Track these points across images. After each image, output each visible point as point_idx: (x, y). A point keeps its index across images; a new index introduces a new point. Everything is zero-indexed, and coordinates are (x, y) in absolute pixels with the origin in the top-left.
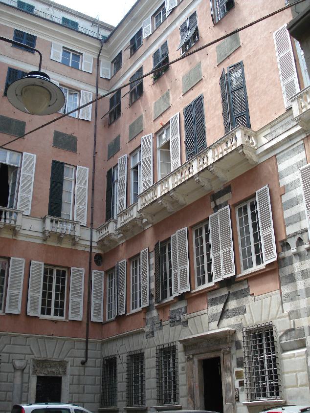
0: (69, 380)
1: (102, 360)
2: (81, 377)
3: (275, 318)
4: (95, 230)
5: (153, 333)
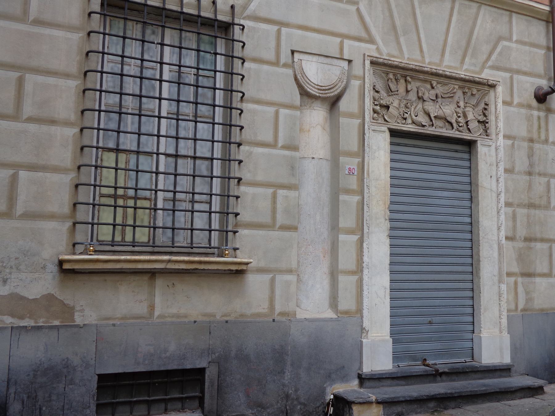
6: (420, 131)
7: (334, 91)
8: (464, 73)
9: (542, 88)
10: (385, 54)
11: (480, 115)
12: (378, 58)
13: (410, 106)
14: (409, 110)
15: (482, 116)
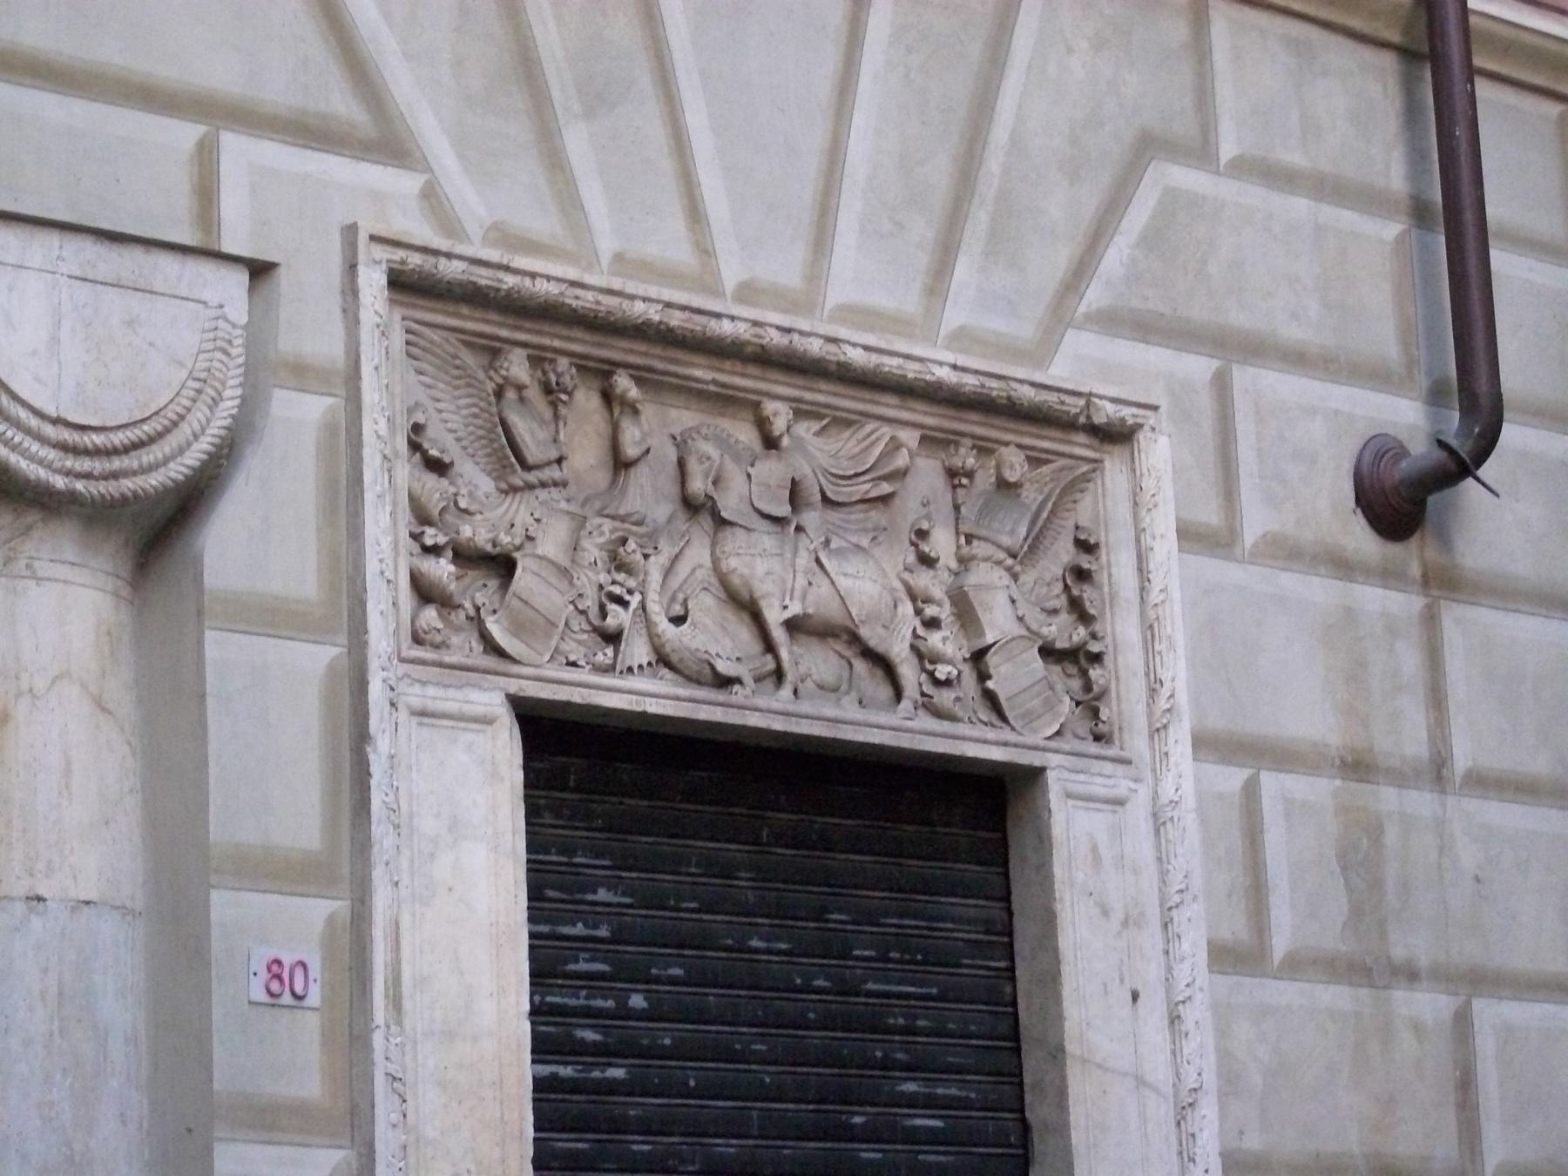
2: (1387, 798)
6: (705, 713)
7: (166, 461)
8: (950, 357)
9: (1401, 452)
10: (474, 229)
11: (1054, 612)
12: (436, 253)
13: (639, 556)
14: (632, 583)
15: (1065, 618)
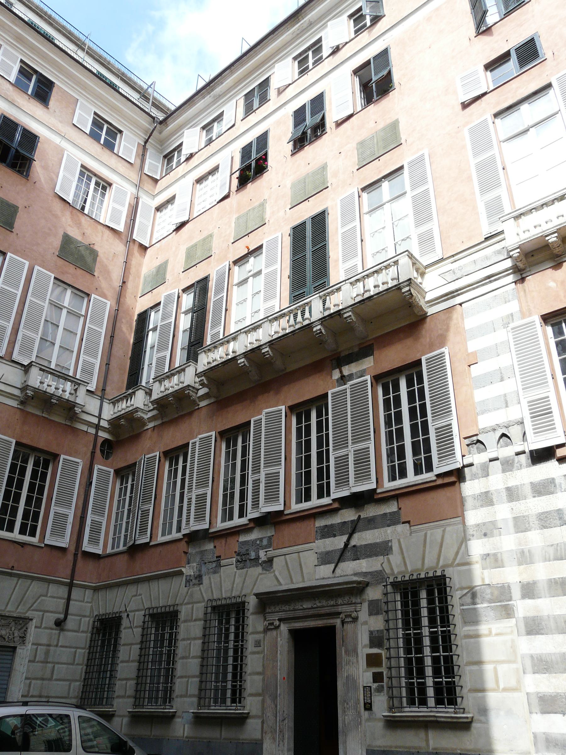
0: (28, 653)
1: (92, 620)
3: (451, 565)
4: (108, 401)
5: (199, 577)
